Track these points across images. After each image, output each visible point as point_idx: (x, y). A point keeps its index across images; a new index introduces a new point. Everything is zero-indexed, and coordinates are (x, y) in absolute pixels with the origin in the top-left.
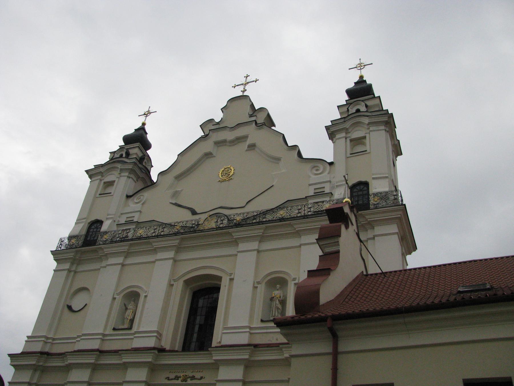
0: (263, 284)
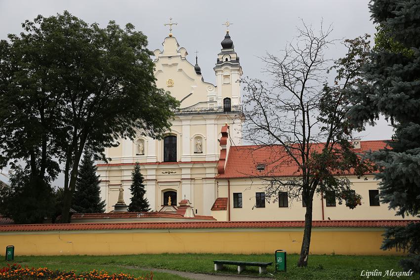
0: (193, 139)
